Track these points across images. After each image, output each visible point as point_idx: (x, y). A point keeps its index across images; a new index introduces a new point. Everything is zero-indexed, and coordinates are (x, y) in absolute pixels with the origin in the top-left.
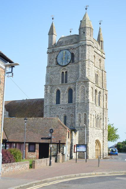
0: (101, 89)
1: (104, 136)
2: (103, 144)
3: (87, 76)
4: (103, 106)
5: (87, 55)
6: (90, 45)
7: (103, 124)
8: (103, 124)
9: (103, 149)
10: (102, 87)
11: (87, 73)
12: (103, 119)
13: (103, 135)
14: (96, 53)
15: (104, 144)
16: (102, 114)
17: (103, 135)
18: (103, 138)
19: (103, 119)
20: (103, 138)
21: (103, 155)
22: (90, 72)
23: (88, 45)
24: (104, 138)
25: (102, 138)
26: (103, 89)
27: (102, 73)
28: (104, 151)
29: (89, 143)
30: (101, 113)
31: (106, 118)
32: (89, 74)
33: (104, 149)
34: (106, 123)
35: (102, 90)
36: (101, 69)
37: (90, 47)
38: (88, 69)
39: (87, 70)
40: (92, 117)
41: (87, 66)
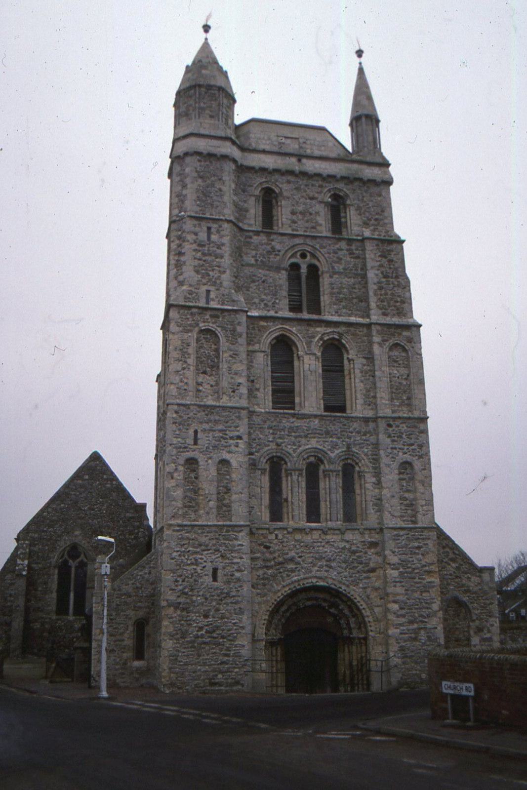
22: (184, 262)
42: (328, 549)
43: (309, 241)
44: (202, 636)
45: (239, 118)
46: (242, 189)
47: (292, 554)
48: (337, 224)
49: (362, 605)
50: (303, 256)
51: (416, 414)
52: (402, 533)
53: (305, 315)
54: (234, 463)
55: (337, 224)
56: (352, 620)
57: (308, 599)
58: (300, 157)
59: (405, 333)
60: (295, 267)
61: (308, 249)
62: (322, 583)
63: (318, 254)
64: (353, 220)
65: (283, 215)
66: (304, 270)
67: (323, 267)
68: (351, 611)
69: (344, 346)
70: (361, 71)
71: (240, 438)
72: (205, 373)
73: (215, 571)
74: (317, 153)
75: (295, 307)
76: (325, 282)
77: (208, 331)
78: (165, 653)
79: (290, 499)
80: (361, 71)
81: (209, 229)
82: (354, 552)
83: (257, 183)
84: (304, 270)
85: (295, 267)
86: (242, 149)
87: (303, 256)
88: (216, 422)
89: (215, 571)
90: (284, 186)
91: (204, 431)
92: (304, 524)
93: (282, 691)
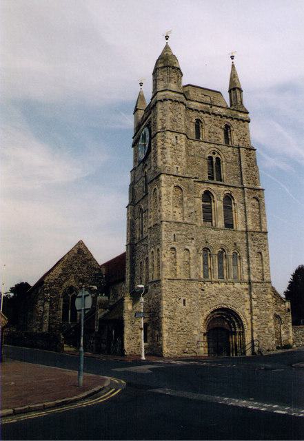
0: (235, 187)
1: (254, 296)
2: (252, 319)
3: (160, 163)
4: (246, 226)
5: (159, 121)
6: (165, 100)
7: (249, 269)
8: (249, 269)
9: (252, 331)
10: (242, 184)
11: (160, 157)
12: (248, 257)
13: (251, 297)
14: (202, 114)
15: (255, 317)
16: (242, 247)
17: (251, 296)
18: (251, 304)
19: (248, 257)
20: (251, 304)
21: (253, 346)
23: (160, 101)
24: (254, 303)
25: (248, 304)
26: (243, 188)
27: (239, 152)
28: (255, 335)
29: (165, 320)
30: (235, 244)
31: (261, 253)
32: (165, 158)
33: (255, 329)
34: (263, 266)
35: (241, 190)
36: (236, 143)
37: (165, 102)
38: (163, 148)
39: (159, 151)
40: (180, 254)
41: (159, 144)
42: (228, 291)
43: (216, 146)
44: (179, 331)
45: (185, 81)
46: (188, 118)
47: (214, 293)
48: (227, 139)
49: (242, 316)
50: (214, 153)
51: (263, 230)
52: (258, 284)
53: (215, 181)
54: (191, 251)
55: (227, 139)
56: (236, 324)
57: (218, 314)
58: (211, 105)
59: (258, 193)
60: (210, 158)
61: (217, 150)
62: (225, 307)
63: (220, 153)
64: (235, 138)
65: (205, 133)
66: (214, 160)
67: (222, 159)
68: (235, 318)
69: (232, 197)
70: (233, 66)
71: (193, 239)
72: (176, 207)
73: (184, 300)
74: (219, 105)
75: (211, 178)
76: (224, 166)
77: (177, 186)
78: (165, 339)
79: (212, 268)
80: (233, 66)
81: (176, 137)
82: (238, 293)
83: (194, 115)
84: (214, 160)
85: (210, 158)
86: (187, 99)
87: (214, 153)
88: (183, 231)
89: (184, 300)
90: (205, 118)
91: (178, 234)
92: (217, 280)
93: (207, 355)
